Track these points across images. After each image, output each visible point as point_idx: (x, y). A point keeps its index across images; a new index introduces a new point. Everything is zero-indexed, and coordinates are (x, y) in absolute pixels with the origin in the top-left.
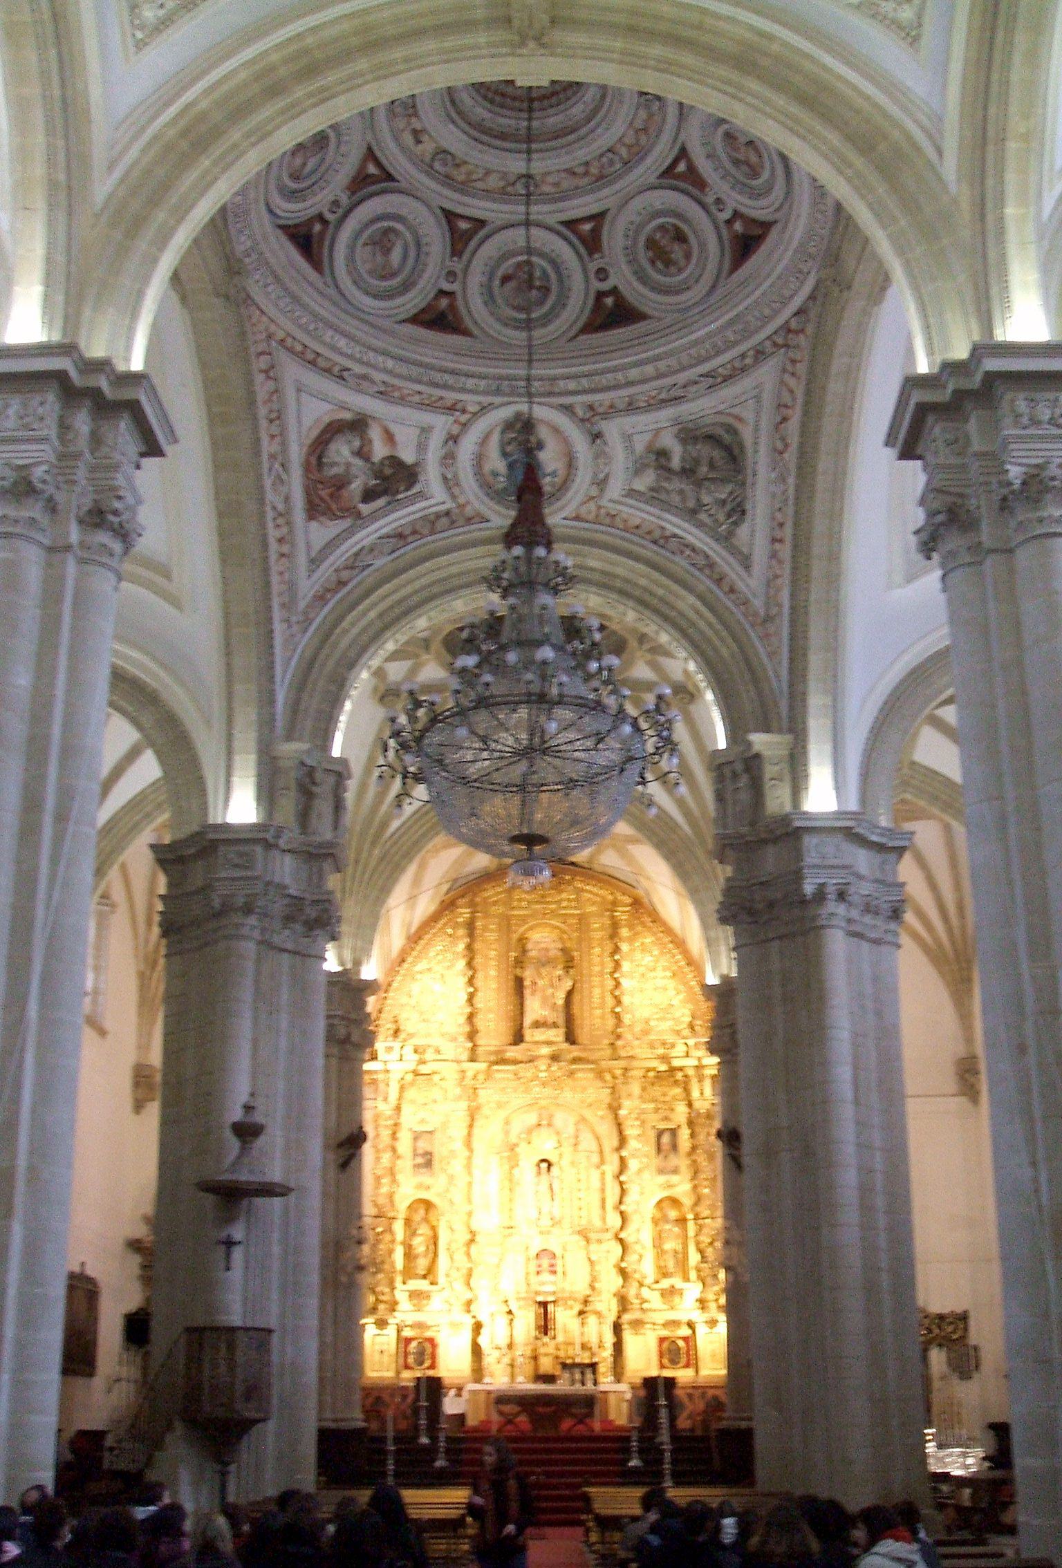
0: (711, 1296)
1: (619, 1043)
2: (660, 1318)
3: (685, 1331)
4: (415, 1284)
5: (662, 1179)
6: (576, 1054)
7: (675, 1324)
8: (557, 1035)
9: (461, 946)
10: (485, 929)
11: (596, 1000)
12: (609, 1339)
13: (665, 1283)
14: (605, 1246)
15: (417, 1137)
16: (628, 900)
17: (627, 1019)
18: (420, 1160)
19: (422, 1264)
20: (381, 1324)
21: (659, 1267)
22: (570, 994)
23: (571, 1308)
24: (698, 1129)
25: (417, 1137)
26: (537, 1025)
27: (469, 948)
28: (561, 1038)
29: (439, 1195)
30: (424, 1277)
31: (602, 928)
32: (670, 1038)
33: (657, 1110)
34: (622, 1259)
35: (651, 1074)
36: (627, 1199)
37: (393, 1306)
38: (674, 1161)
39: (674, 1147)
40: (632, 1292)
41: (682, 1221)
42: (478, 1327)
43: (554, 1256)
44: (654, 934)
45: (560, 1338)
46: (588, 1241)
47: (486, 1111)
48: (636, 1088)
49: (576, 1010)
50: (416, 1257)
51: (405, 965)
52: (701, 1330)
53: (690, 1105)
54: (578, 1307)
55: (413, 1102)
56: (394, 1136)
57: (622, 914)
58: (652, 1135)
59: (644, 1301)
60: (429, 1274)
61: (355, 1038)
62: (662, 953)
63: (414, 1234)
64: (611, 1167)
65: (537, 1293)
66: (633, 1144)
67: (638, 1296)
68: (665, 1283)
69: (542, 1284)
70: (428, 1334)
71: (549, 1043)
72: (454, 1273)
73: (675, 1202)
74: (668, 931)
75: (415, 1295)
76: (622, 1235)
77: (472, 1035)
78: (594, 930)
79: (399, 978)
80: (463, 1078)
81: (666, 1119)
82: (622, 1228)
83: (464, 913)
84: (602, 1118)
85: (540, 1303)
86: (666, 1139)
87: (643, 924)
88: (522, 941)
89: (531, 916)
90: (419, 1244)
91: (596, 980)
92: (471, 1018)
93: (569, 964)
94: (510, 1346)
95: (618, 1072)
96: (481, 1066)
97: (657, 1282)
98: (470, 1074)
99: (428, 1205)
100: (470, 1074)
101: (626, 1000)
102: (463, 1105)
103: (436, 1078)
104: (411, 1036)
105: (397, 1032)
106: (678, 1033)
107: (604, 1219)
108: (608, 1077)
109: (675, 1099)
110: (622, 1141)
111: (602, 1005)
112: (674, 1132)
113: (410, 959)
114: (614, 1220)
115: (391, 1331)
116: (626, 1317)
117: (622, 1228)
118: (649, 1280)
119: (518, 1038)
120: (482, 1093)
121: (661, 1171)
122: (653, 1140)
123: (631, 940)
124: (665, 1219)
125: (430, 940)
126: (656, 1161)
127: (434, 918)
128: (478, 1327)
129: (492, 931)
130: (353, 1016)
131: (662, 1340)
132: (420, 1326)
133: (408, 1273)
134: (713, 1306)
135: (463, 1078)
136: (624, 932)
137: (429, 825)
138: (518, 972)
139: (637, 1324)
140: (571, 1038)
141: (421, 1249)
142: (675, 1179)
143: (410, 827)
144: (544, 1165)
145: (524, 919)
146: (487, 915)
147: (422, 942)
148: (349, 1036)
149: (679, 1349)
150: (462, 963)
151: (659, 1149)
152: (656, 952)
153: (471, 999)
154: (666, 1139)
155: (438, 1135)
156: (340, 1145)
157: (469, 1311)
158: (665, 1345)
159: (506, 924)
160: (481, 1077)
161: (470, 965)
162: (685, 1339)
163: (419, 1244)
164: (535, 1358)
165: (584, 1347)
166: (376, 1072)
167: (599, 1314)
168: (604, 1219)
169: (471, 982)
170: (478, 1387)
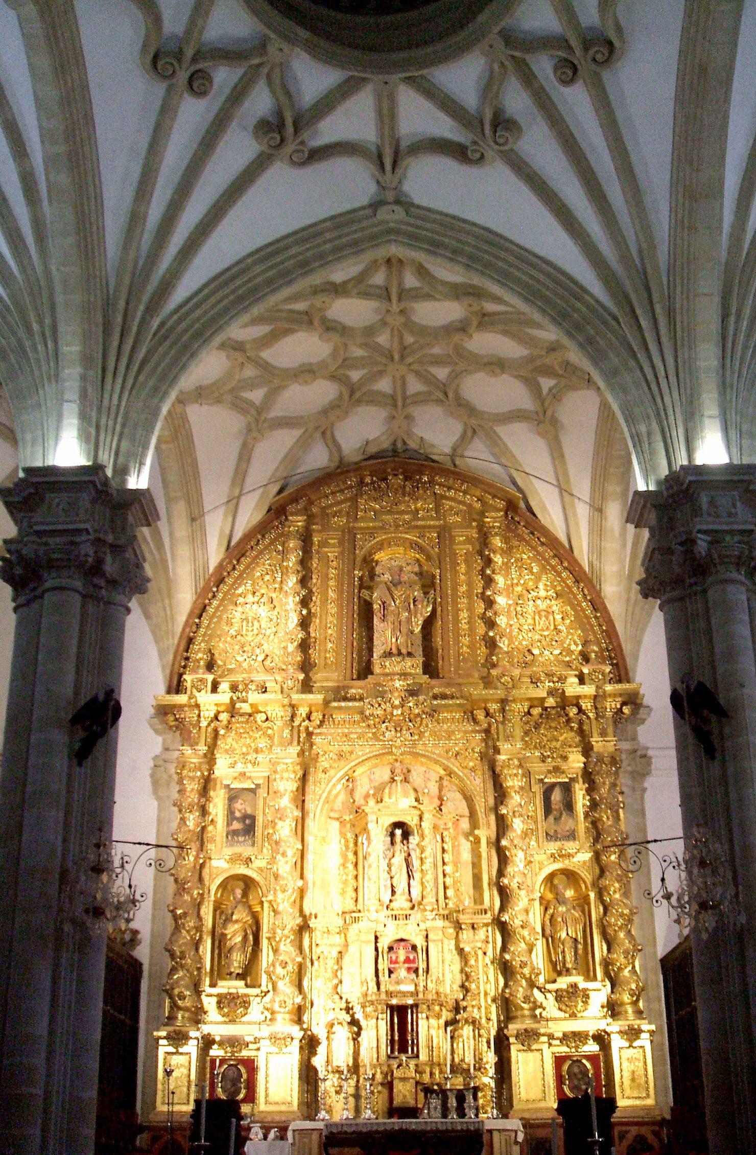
0: (626, 998)
1: (494, 672)
2: (559, 1028)
3: (592, 1047)
4: (227, 986)
5: (553, 847)
6: (436, 690)
7: (578, 1037)
8: (413, 666)
9: (292, 561)
10: (324, 543)
11: (464, 625)
12: (490, 1058)
13: (563, 983)
14: (481, 934)
15: (233, 796)
16: (501, 504)
17: (503, 645)
18: (236, 825)
19: (237, 961)
20: (178, 1038)
21: (554, 964)
22: (428, 624)
23: (438, 1016)
24: (599, 779)
25: (233, 796)
26: (388, 654)
27: (304, 562)
28: (419, 670)
29: (261, 869)
30: (241, 976)
31: (469, 540)
32: (559, 671)
33: (543, 759)
34: (504, 949)
35: (536, 711)
36: (510, 869)
37: (197, 1016)
38: (567, 823)
39: (569, 806)
40: (520, 991)
41: (583, 903)
42: (310, 1044)
43: (414, 948)
44: (534, 548)
45: (423, 1057)
46: (458, 926)
47: (323, 763)
48: (516, 726)
49: (438, 641)
50: (230, 950)
51: (224, 588)
52: (617, 1043)
53: (587, 750)
54: (446, 1015)
55: (229, 752)
56: (205, 791)
57: (495, 519)
58: (537, 789)
59: (536, 1006)
60: (247, 974)
61: (110, 566)
62: (543, 569)
63: (228, 920)
64: (486, 833)
65: (390, 994)
66: (515, 799)
67: (527, 999)
68: (563, 983)
69: (398, 983)
70: (245, 1053)
71: (404, 675)
72: (279, 971)
73: (570, 876)
74: (552, 542)
75: (228, 1003)
76: (505, 918)
77: (306, 666)
78: (460, 543)
79: (215, 603)
80: (293, 717)
81: (557, 770)
82: (502, 909)
83: (298, 522)
84: (473, 769)
85: (392, 1008)
86: (556, 796)
87: (521, 539)
88: (369, 563)
89: (382, 528)
90: (234, 934)
91: (463, 602)
92: (304, 646)
93: (428, 584)
94: (355, 1068)
95: (494, 707)
96: (317, 698)
97: (554, 981)
98: (303, 711)
99: (248, 883)
100: (303, 711)
101: (502, 621)
102: (294, 750)
103: (260, 717)
104: (230, 671)
105: (210, 666)
106: (568, 665)
107: (479, 899)
108: (480, 715)
109: (564, 744)
110: (501, 794)
111: (472, 629)
112: (567, 788)
113: (230, 581)
114: (492, 899)
115: (192, 1048)
116: (513, 1028)
117: (502, 909)
118: (541, 980)
119: (365, 671)
120: (317, 740)
121: (550, 837)
122: (539, 800)
123: (508, 552)
124: (560, 900)
125: (256, 557)
126: (542, 826)
127: (262, 529)
128: (310, 1044)
129: (333, 546)
130: (110, 538)
131: (559, 1061)
132: (234, 1042)
133: (219, 972)
134: (630, 1009)
135: (293, 717)
136: (497, 542)
137: (232, 297)
138: (365, 593)
139: (529, 1037)
140: (430, 669)
141: (238, 939)
142: (570, 846)
143: (207, 297)
144: (398, 832)
145: (372, 532)
146: (325, 528)
147: (245, 561)
148: (100, 562)
149: (585, 1072)
150: (292, 581)
151: (548, 809)
152: (535, 570)
153: (304, 624)
154: (556, 796)
155: (262, 792)
156: (77, 720)
157: (299, 1021)
158: (565, 1067)
159: (350, 537)
160: (317, 717)
161: (304, 581)
162: (592, 1058)
163: (234, 934)
164: (390, 1086)
165: (455, 1069)
166: (181, 707)
167: (474, 1022)
168: (479, 899)
169: (305, 602)
170: (308, 1125)
